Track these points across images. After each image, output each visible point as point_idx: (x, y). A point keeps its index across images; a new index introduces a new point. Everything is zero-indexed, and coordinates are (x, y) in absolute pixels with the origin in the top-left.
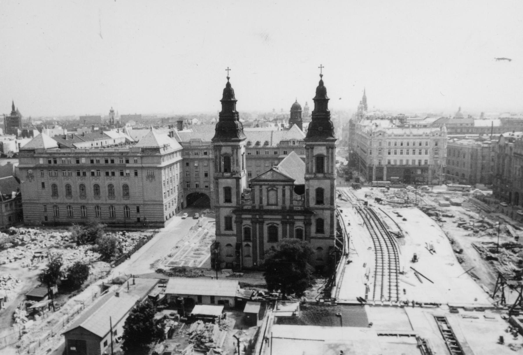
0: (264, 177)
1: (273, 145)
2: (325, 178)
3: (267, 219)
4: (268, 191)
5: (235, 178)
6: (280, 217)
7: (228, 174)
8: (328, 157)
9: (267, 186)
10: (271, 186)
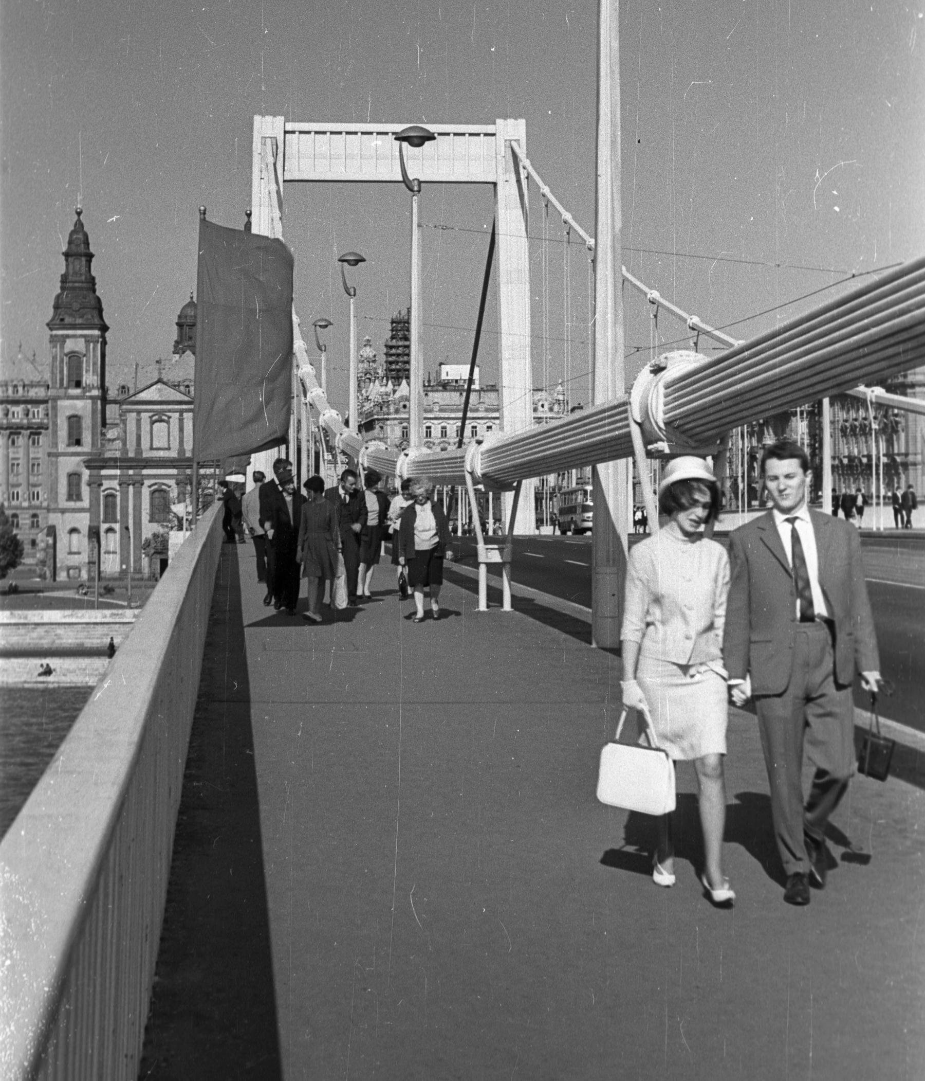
0: (144, 396)
3: (149, 477)
7: (78, 391)
9: (151, 414)
10: (157, 412)
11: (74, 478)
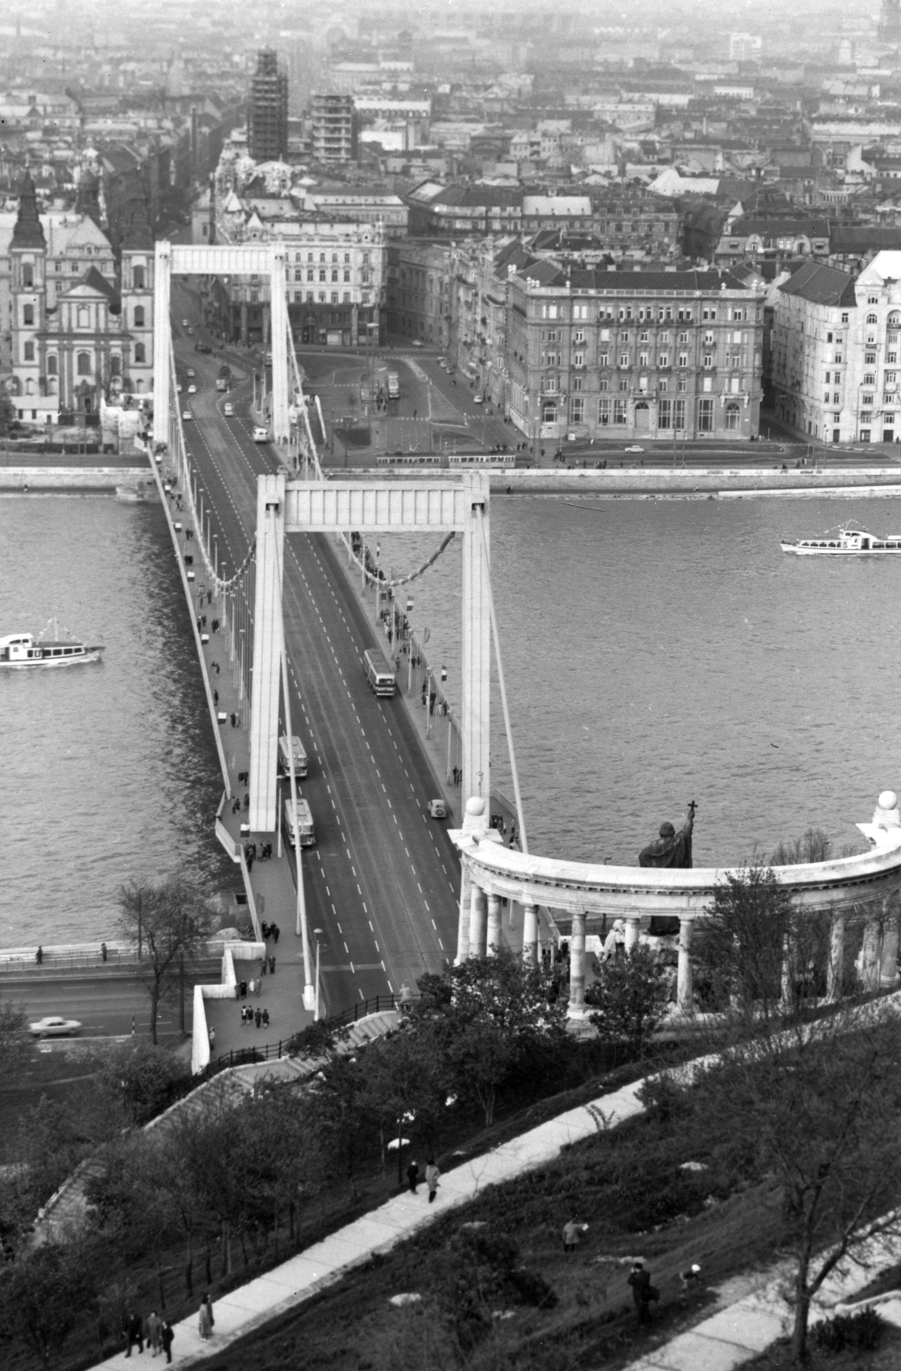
2: (145, 294)
4: (79, 310)
6: (92, 342)
8: (147, 268)
11: (29, 346)
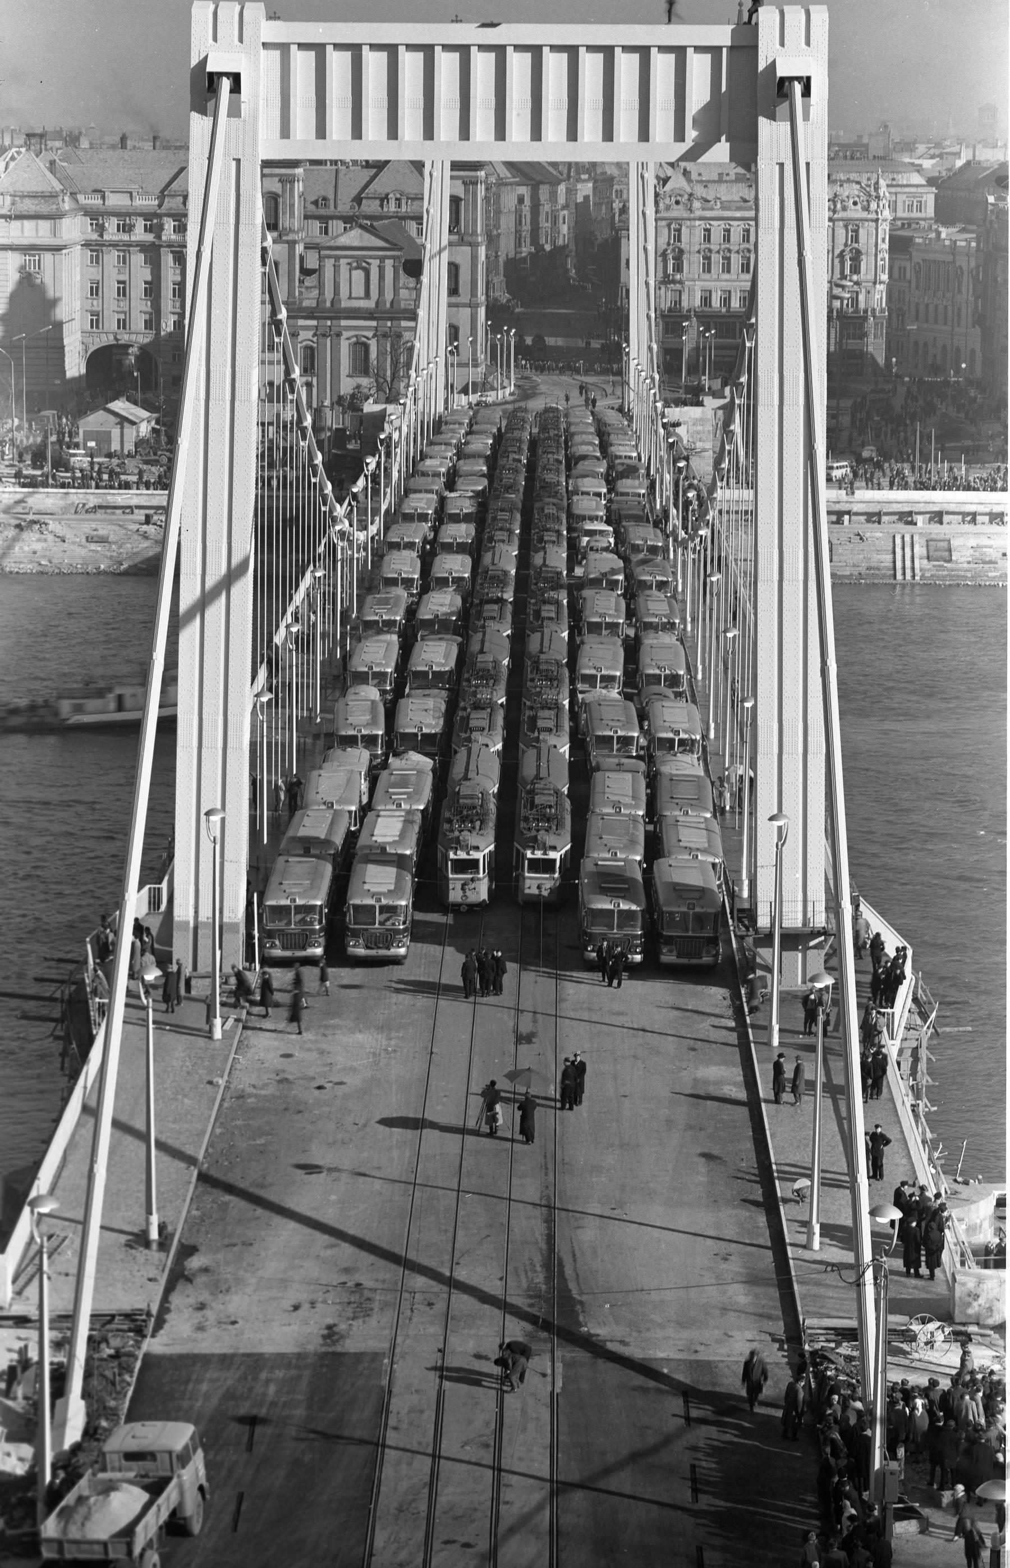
1: (339, 209)
3: (348, 328)
5: (288, 242)
10: (358, 259)
